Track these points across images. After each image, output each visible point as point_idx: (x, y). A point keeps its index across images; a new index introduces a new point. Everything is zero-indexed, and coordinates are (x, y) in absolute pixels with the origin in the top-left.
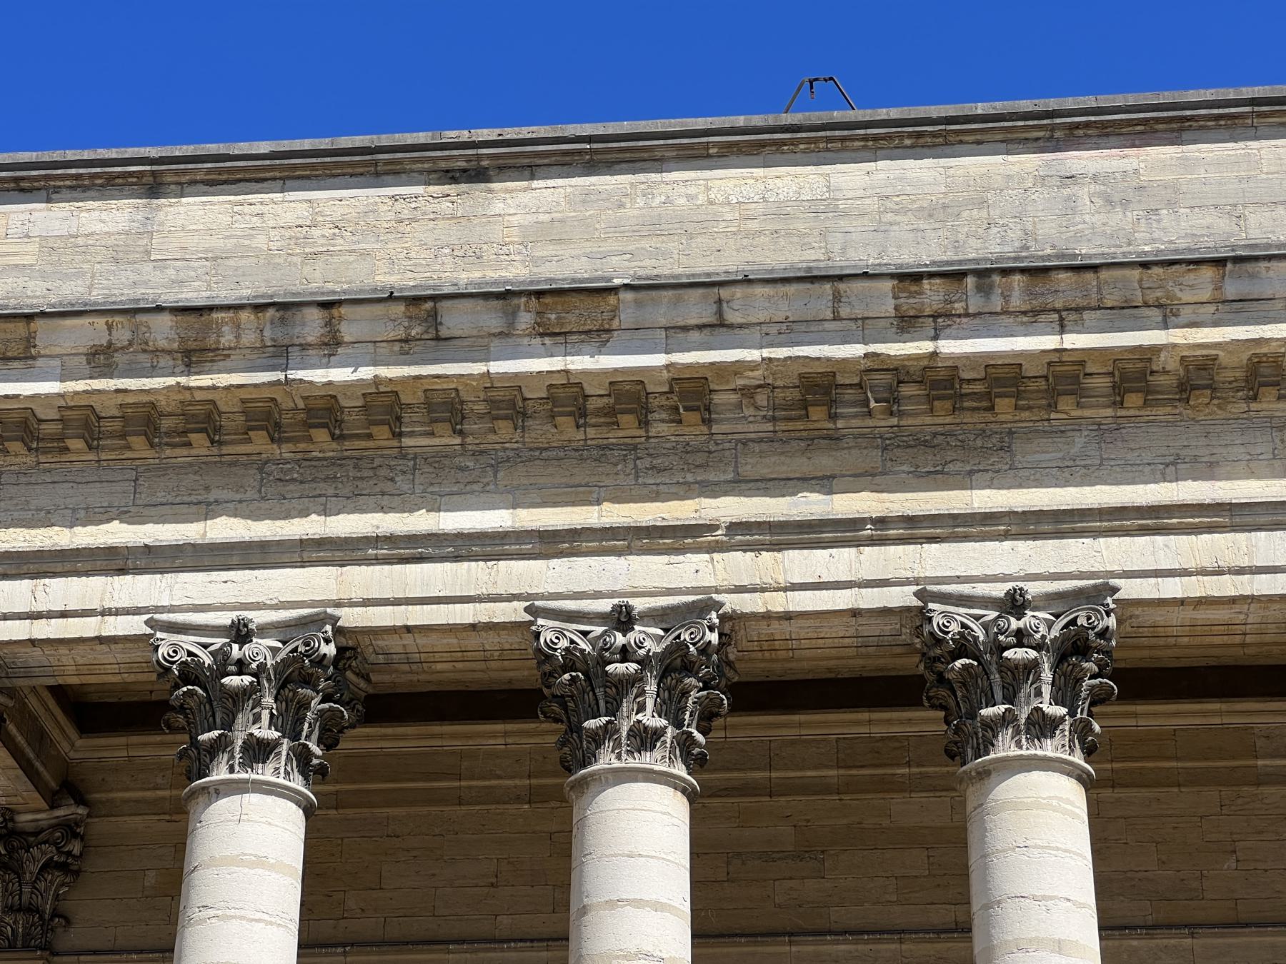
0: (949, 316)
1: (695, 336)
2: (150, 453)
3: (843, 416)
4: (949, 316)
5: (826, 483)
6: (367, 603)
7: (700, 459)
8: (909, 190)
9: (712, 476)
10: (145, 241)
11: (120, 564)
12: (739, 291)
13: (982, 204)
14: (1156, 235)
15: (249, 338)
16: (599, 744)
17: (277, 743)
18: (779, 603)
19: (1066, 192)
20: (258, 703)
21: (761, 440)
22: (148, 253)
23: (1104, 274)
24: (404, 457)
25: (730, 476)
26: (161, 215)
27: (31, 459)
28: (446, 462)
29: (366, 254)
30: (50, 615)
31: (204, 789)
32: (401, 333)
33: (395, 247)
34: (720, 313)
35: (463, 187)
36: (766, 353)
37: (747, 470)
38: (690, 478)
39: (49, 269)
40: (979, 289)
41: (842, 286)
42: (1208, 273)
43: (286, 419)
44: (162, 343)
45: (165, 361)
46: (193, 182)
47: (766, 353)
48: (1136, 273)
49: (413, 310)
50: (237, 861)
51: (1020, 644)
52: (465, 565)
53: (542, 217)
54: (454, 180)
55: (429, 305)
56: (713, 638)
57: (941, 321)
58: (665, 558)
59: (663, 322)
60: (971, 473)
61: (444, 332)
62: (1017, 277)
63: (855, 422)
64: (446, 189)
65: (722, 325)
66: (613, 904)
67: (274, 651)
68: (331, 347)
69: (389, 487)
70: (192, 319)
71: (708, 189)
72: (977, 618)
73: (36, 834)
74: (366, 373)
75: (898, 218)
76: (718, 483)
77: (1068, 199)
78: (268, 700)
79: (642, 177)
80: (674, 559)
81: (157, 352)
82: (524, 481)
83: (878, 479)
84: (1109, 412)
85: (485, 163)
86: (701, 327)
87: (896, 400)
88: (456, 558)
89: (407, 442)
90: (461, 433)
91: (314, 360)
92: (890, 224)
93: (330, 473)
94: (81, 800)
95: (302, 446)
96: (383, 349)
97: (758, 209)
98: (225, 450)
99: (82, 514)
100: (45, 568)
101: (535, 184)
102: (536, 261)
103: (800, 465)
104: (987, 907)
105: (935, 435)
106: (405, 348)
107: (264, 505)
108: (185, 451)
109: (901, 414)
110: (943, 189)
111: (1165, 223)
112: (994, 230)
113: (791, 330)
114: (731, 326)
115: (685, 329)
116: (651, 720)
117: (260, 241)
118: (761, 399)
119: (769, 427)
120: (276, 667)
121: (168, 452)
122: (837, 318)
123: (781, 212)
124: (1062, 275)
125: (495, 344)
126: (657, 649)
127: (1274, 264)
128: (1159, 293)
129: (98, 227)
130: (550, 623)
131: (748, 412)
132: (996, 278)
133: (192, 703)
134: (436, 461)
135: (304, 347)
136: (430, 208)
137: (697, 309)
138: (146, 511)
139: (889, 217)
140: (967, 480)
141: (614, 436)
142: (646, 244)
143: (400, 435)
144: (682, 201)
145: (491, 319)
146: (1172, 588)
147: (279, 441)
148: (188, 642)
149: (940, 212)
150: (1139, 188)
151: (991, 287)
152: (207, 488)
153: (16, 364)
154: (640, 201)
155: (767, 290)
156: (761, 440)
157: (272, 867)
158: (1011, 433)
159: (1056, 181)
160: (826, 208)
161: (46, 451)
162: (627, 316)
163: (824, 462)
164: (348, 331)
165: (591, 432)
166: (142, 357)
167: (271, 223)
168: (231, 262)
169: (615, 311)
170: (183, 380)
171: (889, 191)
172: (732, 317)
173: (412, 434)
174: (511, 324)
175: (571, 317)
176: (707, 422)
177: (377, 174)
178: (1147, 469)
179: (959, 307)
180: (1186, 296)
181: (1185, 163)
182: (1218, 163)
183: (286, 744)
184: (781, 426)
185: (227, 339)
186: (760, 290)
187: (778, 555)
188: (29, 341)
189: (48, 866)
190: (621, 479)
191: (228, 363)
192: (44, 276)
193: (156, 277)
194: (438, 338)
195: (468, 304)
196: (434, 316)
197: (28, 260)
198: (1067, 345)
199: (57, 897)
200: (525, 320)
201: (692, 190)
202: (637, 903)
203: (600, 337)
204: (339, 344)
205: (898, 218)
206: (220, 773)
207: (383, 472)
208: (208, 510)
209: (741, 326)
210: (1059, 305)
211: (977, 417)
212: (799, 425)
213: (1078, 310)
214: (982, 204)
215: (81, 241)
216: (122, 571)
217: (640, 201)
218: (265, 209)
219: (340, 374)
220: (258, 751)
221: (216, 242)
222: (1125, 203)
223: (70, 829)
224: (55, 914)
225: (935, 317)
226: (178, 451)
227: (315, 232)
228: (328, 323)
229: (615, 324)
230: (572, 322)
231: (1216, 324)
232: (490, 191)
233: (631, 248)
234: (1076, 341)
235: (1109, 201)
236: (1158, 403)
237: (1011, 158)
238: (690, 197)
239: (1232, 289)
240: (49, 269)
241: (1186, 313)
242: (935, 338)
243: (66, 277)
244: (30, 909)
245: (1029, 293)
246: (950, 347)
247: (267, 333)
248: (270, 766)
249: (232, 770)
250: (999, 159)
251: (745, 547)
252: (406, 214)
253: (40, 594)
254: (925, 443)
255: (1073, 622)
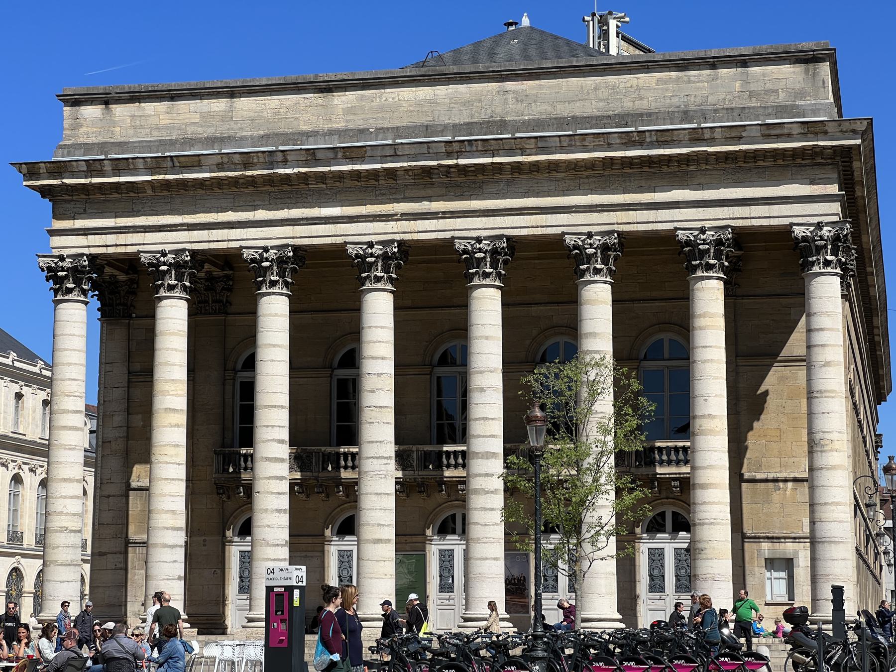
0: (461, 152)
1: (389, 158)
2: (237, 190)
3: (434, 178)
4: (461, 152)
5: (430, 199)
6: (301, 237)
7: (394, 191)
8: (458, 96)
9: (397, 197)
10: (231, 114)
11: (232, 226)
12: (400, 147)
13: (480, 101)
14: (530, 112)
15: (262, 160)
16: (366, 280)
17: (279, 280)
18: (416, 237)
19: (505, 97)
20: (272, 269)
21: (411, 185)
22: (232, 118)
23: (504, 141)
24: (310, 190)
25: (402, 196)
26: (235, 105)
27: (204, 192)
28: (322, 192)
29: (296, 119)
30: (214, 241)
31: (260, 293)
32: (305, 158)
33: (306, 117)
34: (395, 152)
35: (325, 94)
36: (409, 164)
37: (407, 195)
38: (391, 197)
39: (203, 124)
40: (469, 145)
41: (430, 145)
42: (533, 140)
43: (275, 180)
44: (237, 162)
45: (238, 167)
46: (244, 93)
47: (409, 164)
48: (513, 141)
49: (308, 152)
50: (270, 315)
51: (480, 252)
52: (328, 225)
53: (350, 105)
54: (322, 92)
55: (312, 151)
56: (396, 250)
57: (459, 154)
58: (384, 223)
59: (380, 155)
60: (471, 195)
61: (317, 158)
62: (479, 142)
63: (437, 180)
64: (320, 95)
65: (397, 155)
66: (370, 327)
67: (276, 254)
68: (285, 163)
69: (305, 200)
70: (245, 155)
71: (398, 95)
72: (469, 243)
73: (219, 278)
74: (296, 170)
75: (455, 106)
76: (399, 199)
77: (506, 99)
78: (275, 268)
79: (378, 91)
80: (386, 223)
81: (236, 164)
82: (344, 198)
83: (444, 197)
84: (510, 176)
85: (331, 86)
86: (390, 156)
87: (449, 173)
88: (326, 224)
89: (310, 186)
90: (326, 184)
91: (281, 166)
92: (452, 108)
93: (289, 196)
94: (231, 268)
95: (280, 188)
96: (300, 163)
97: (412, 103)
98: (258, 189)
99: (220, 209)
100: (211, 227)
101: (347, 93)
102: (347, 121)
103: (423, 193)
104: (470, 326)
105: (461, 183)
106: (307, 164)
107: (271, 206)
108: (247, 189)
109: (451, 177)
110: (468, 95)
111: (533, 108)
112: (483, 110)
113: (416, 157)
114: (399, 155)
115: (386, 156)
116: (380, 274)
117: (265, 114)
118: (410, 173)
119: (413, 181)
120: (276, 258)
121: (242, 190)
122: (429, 153)
123: (420, 103)
124: (492, 141)
125: (332, 161)
126: (381, 253)
127: (551, 138)
128: (520, 146)
129: (216, 109)
130: (351, 246)
131: (408, 177)
132: (473, 142)
133: (255, 268)
134: (319, 192)
135: (278, 162)
136: (315, 102)
137: (389, 152)
138: (238, 208)
139: (452, 105)
140: (469, 198)
141: (369, 184)
142: (379, 115)
143: (308, 184)
144: (391, 100)
145: (331, 155)
146: (524, 232)
147: (274, 186)
148: (251, 251)
149: (467, 103)
150: (527, 96)
151: (472, 144)
152: (254, 201)
153: (196, 168)
154: (378, 99)
155: (408, 146)
156: (411, 185)
157: (279, 316)
158: (483, 182)
159: (502, 93)
160: (433, 102)
161: (208, 190)
162: (369, 153)
163: (429, 192)
164: (289, 158)
165: (363, 183)
166: (232, 165)
167: (268, 107)
168: (256, 121)
169: (366, 151)
170: (244, 172)
171: (452, 96)
172: (399, 153)
173: (311, 184)
174: (336, 156)
175: (353, 154)
176: (396, 180)
177: (299, 90)
178: (520, 194)
179: (463, 150)
180: (527, 147)
181: (541, 87)
182: (550, 87)
183: (281, 280)
184: (416, 181)
185: (255, 161)
186: (406, 146)
187: (415, 222)
188: (200, 161)
189: (223, 289)
190: (371, 198)
191: (255, 168)
192: (202, 126)
193: (235, 126)
194: (316, 160)
195: (324, 150)
196: (314, 153)
197: (197, 120)
198: (494, 161)
199: (227, 296)
200: (340, 155)
201: (393, 96)
202: (376, 327)
203: (362, 159)
204: (288, 161)
205: (455, 106)
206: (264, 290)
207: (304, 196)
208: (255, 208)
209: (402, 155)
210: (492, 149)
211: (473, 178)
212: (422, 181)
213: (498, 150)
214: (480, 101)
215: (212, 114)
216: (232, 228)
217: (378, 99)
218: (266, 102)
219: (289, 171)
220: (273, 284)
221: (252, 114)
222: (522, 101)
223: (228, 277)
224: (227, 301)
225: (457, 152)
226: (245, 190)
227: (282, 110)
228: (284, 156)
229: (366, 155)
230: (353, 155)
231: (536, 154)
232: (333, 96)
233: (375, 116)
234: (497, 160)
235: (517, 100)
236: (524, 174)
237: (490, 84)
238: (393, 98)
239: (540, 145)
240: (203, 124)
241: (528, 151)
242: (457, 159)
243: (209, 126)
244: (220, 301)
245: (483, 146)
246: (462, 162)
247: (267, 159)
248: (277, 287)
249: (266, 288)
250: (485, 84)
251: (406, 220)
252: (308, 104)
253: (210, 235)
254: (457, 186)
255: (495, 245)
